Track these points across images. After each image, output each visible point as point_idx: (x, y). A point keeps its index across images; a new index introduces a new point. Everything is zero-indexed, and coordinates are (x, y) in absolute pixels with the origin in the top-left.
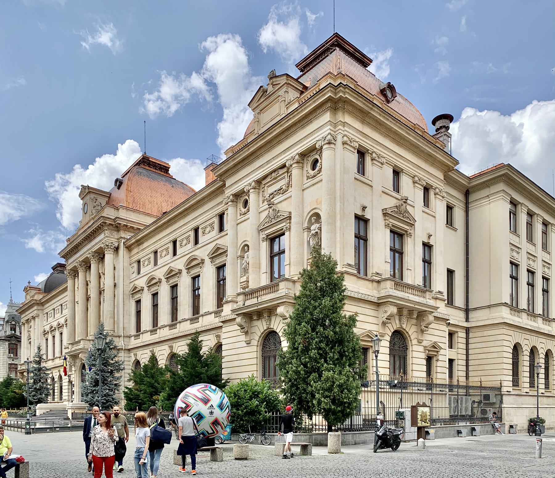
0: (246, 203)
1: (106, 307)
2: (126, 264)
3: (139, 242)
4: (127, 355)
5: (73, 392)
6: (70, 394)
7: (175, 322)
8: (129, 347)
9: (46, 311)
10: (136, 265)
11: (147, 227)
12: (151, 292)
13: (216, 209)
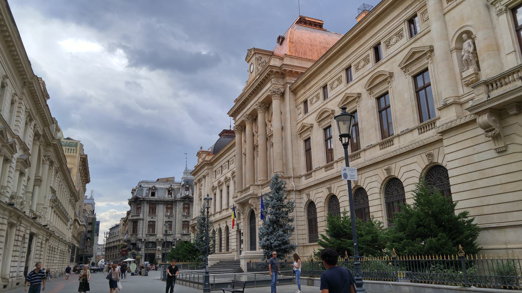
1: (276, 150)
2: (293, 107)
3: (304, 84)
4: (298, 196)
5: (241, 242)
6: (239, 243)
7: (331, 163)
8: (300, 188)
9: (214, 169)
10: (302, 106)
11: (308, 69)
12: (322, 127)
13: (404, 14)
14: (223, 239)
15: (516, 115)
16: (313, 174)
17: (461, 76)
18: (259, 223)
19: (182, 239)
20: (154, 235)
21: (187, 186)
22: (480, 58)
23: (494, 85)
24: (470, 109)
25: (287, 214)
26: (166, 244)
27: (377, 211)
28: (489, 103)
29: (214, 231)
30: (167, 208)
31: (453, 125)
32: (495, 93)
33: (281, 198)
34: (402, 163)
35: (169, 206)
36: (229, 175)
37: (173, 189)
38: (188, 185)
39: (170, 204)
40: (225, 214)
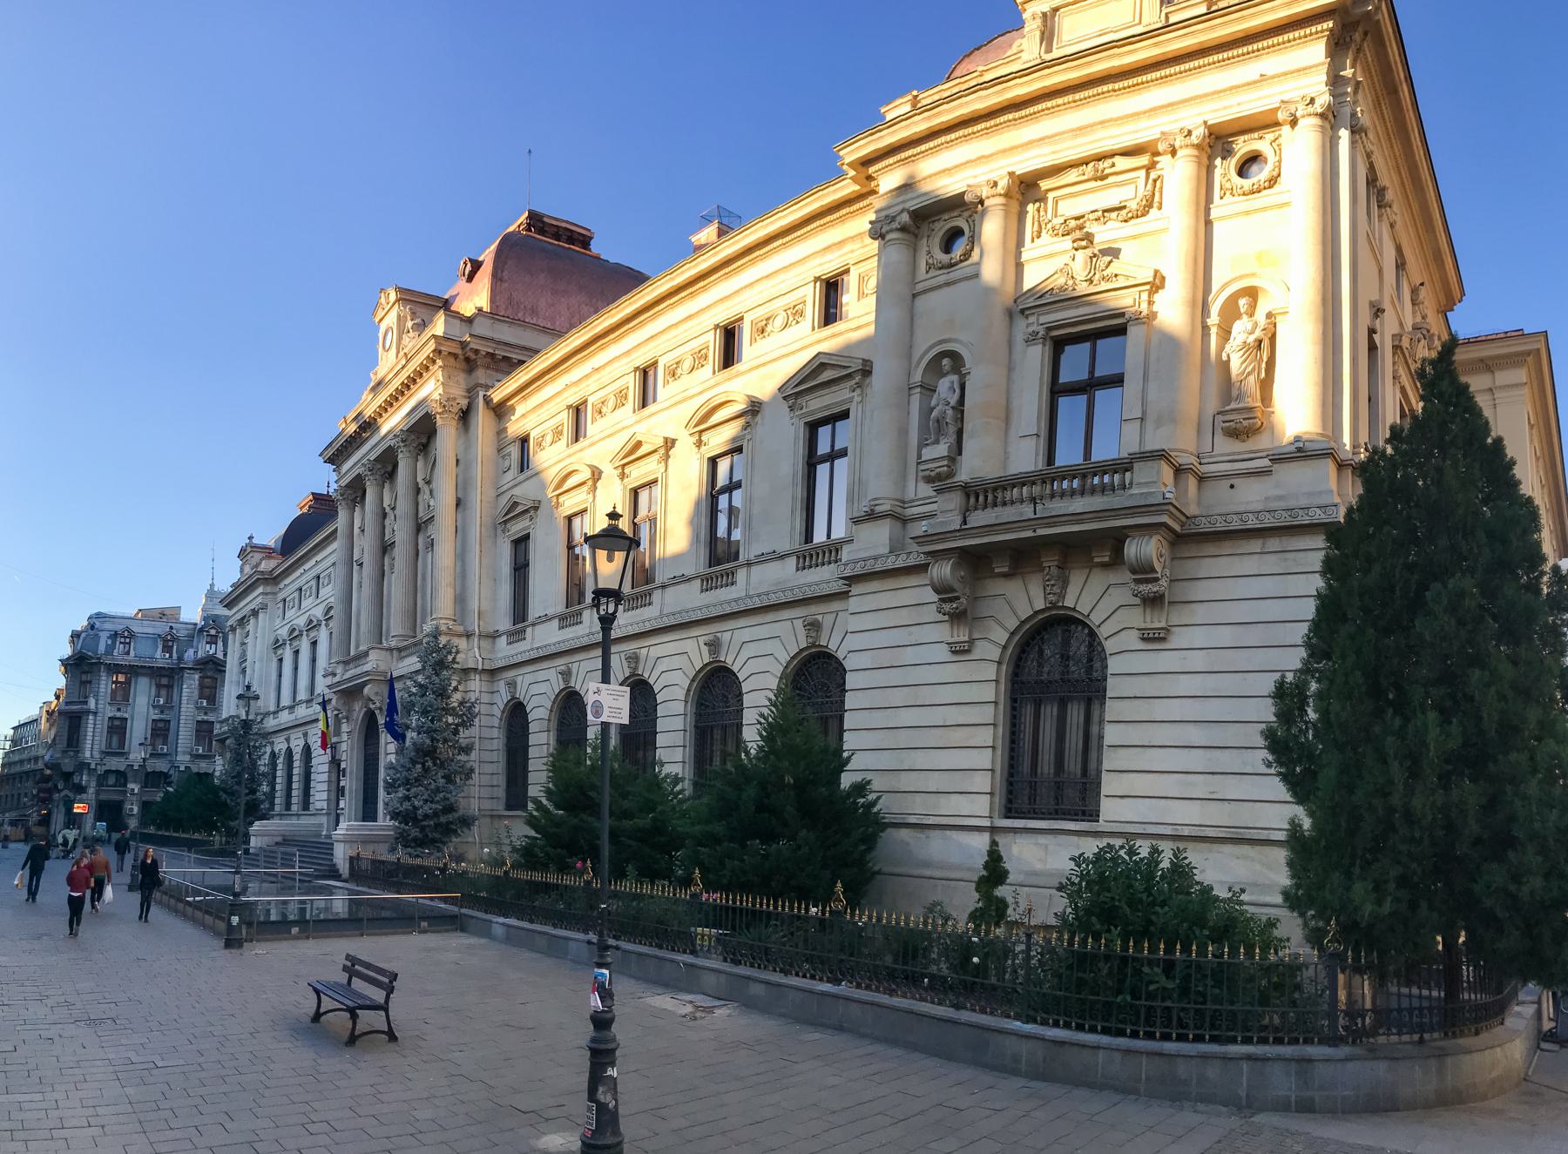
14: (295, 778)
15: (1005, 576)
16: (529, 630)
17: (919, 456)
18: (388, 749)
19: (195, 769)
20: (122, 754)
21: (213, 632)
22: (968, 427)
23: (981, 498)
24: (920, 540)
25: (456, 732)
26: (154, 779)
27: (673, 752)
28: (964, 537)
29: (273, 755)
30: (159, 686)
31: (879, 567)
32: (979, 518)
33: (445, 689)
34: (746, 635)
35: (164, 681)
36: (318, 613)
37: (174, 639)
38: (213, 628)
39: (166, 678)
40: (302, 712)
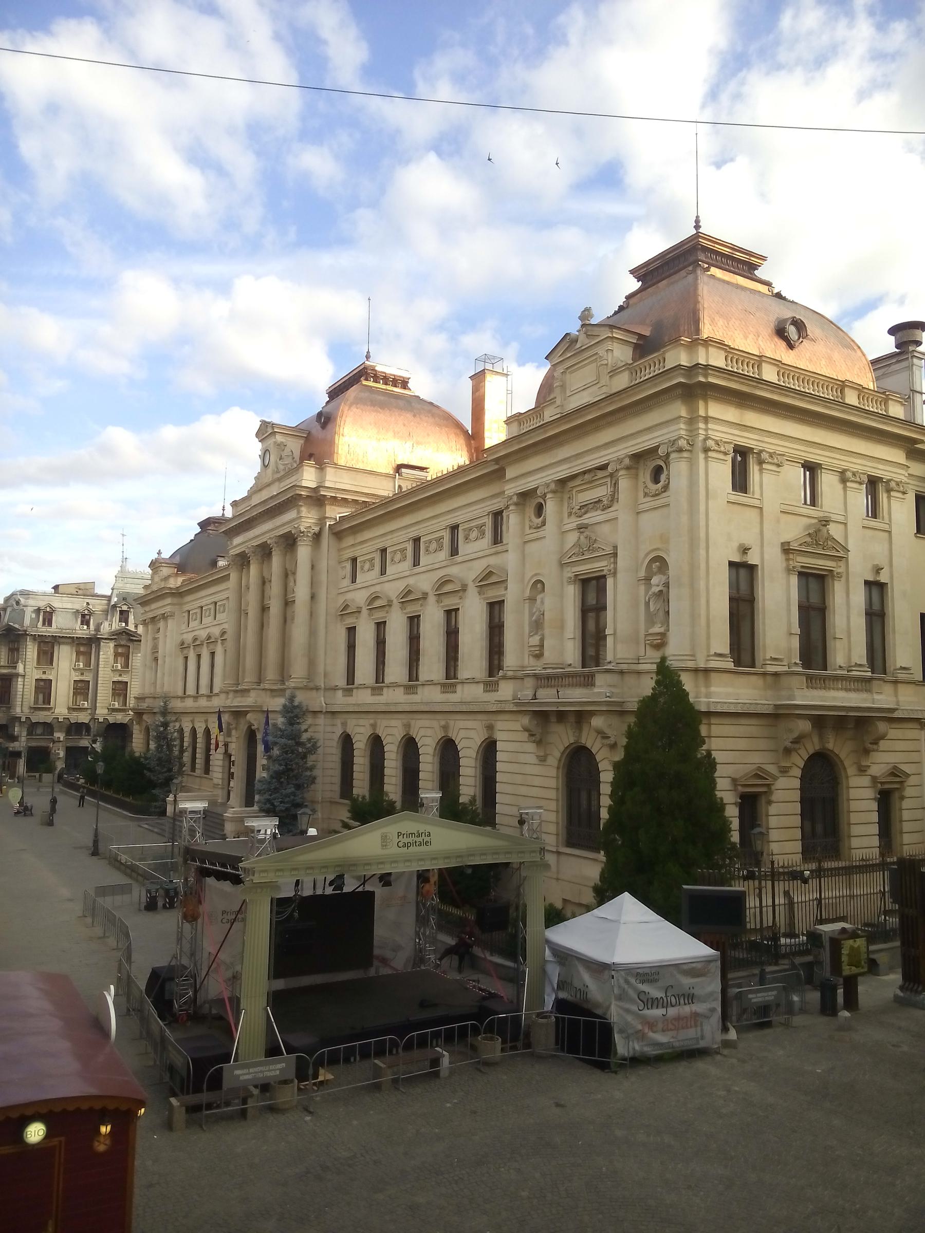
0: (539, 510)
